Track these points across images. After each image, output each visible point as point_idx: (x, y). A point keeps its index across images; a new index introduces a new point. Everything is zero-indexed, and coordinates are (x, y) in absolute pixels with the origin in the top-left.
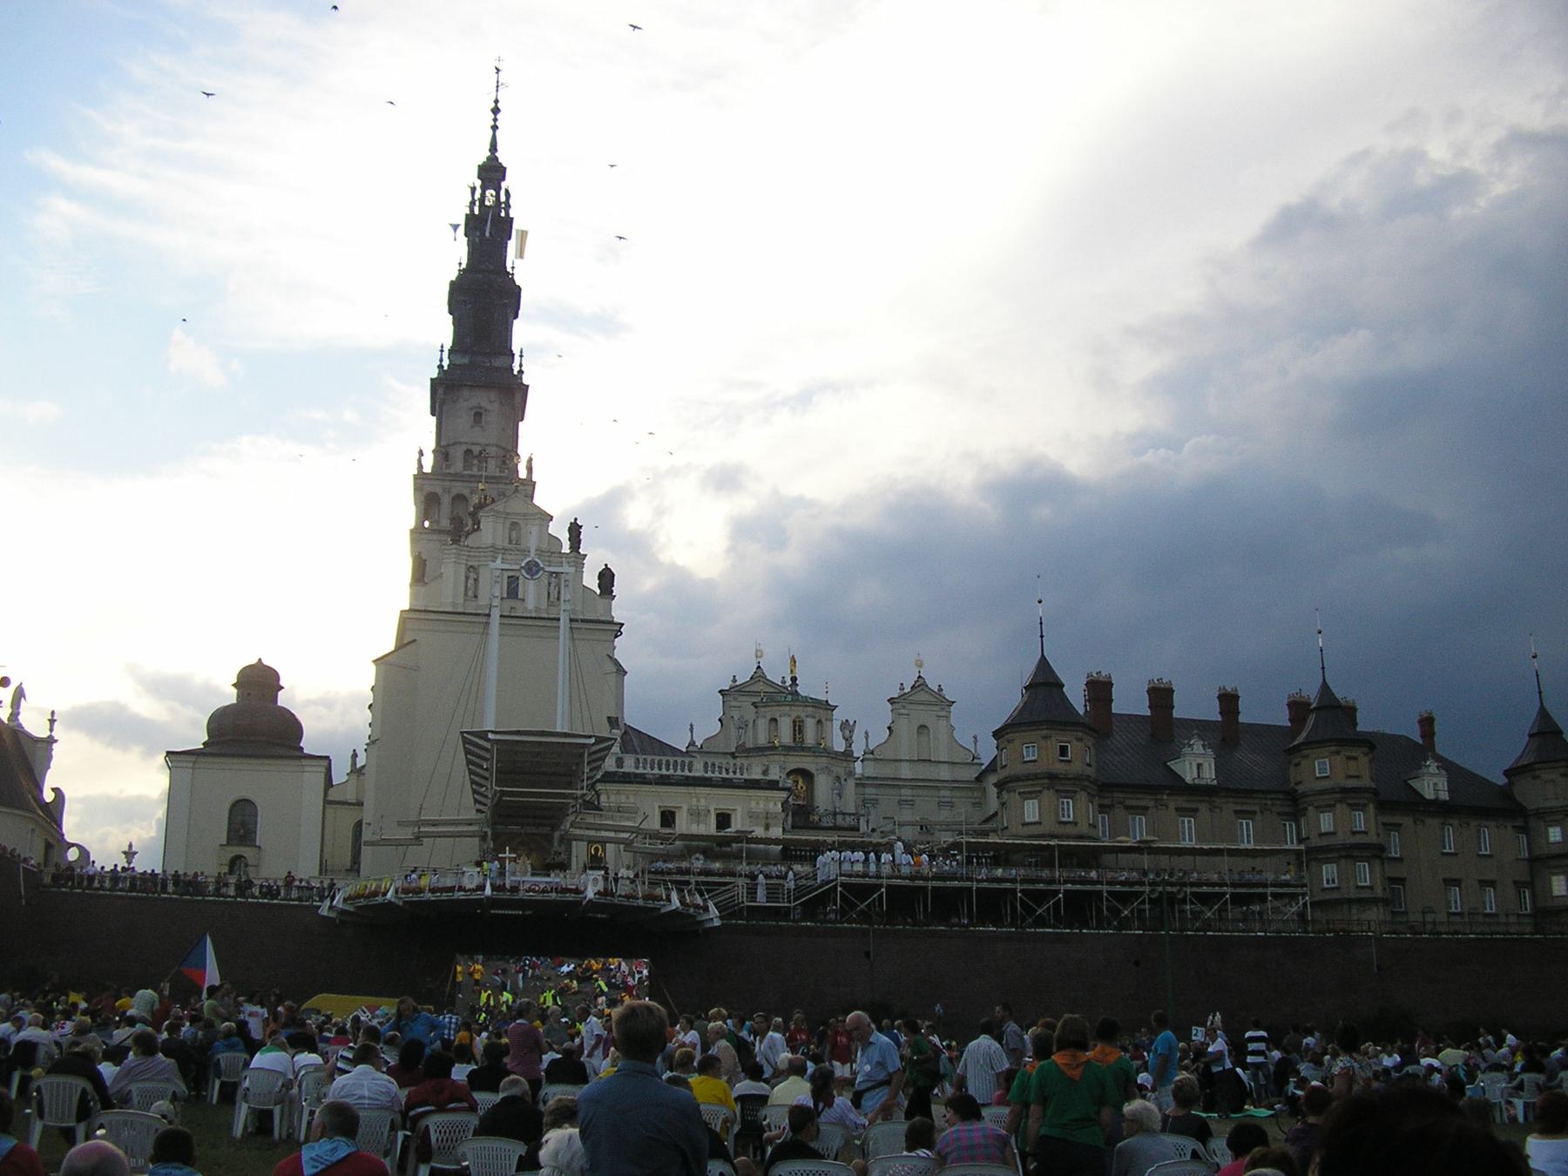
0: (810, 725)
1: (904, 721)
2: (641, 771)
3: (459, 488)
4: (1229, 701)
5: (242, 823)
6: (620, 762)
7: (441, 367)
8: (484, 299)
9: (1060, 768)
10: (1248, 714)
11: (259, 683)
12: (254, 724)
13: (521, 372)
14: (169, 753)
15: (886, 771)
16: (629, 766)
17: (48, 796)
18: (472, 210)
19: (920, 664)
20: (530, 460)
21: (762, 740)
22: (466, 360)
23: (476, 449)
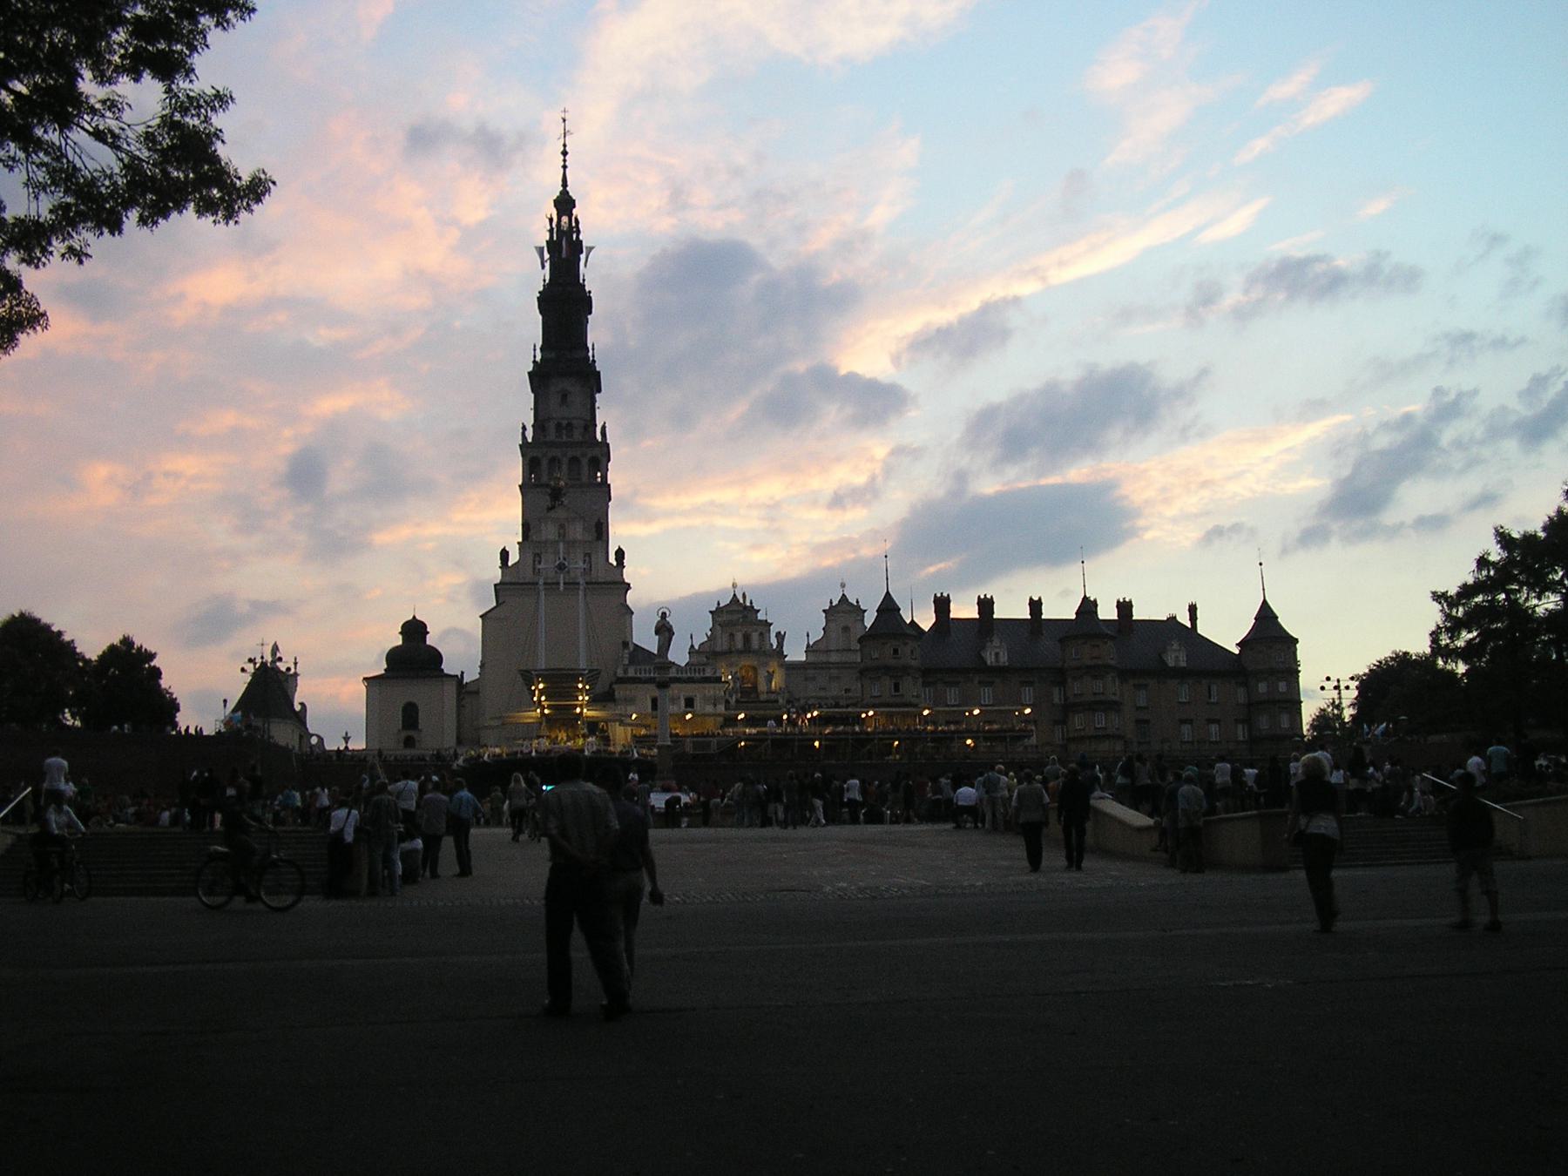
0: (755, 637)
1: (832, 625)
3: (556, 452)
4: (1036, 606)
5: (410, 715)
6: (625, 671)
8: (565, 303)
9: (892, 662)
10: (1048, 613)
11: (414, 630)
12: (414, 655)
15: (823, 658)
16: (631, 673)
17: (298, 708)
19: (843, 586)
20: (604, 428)
21: (725, 647)
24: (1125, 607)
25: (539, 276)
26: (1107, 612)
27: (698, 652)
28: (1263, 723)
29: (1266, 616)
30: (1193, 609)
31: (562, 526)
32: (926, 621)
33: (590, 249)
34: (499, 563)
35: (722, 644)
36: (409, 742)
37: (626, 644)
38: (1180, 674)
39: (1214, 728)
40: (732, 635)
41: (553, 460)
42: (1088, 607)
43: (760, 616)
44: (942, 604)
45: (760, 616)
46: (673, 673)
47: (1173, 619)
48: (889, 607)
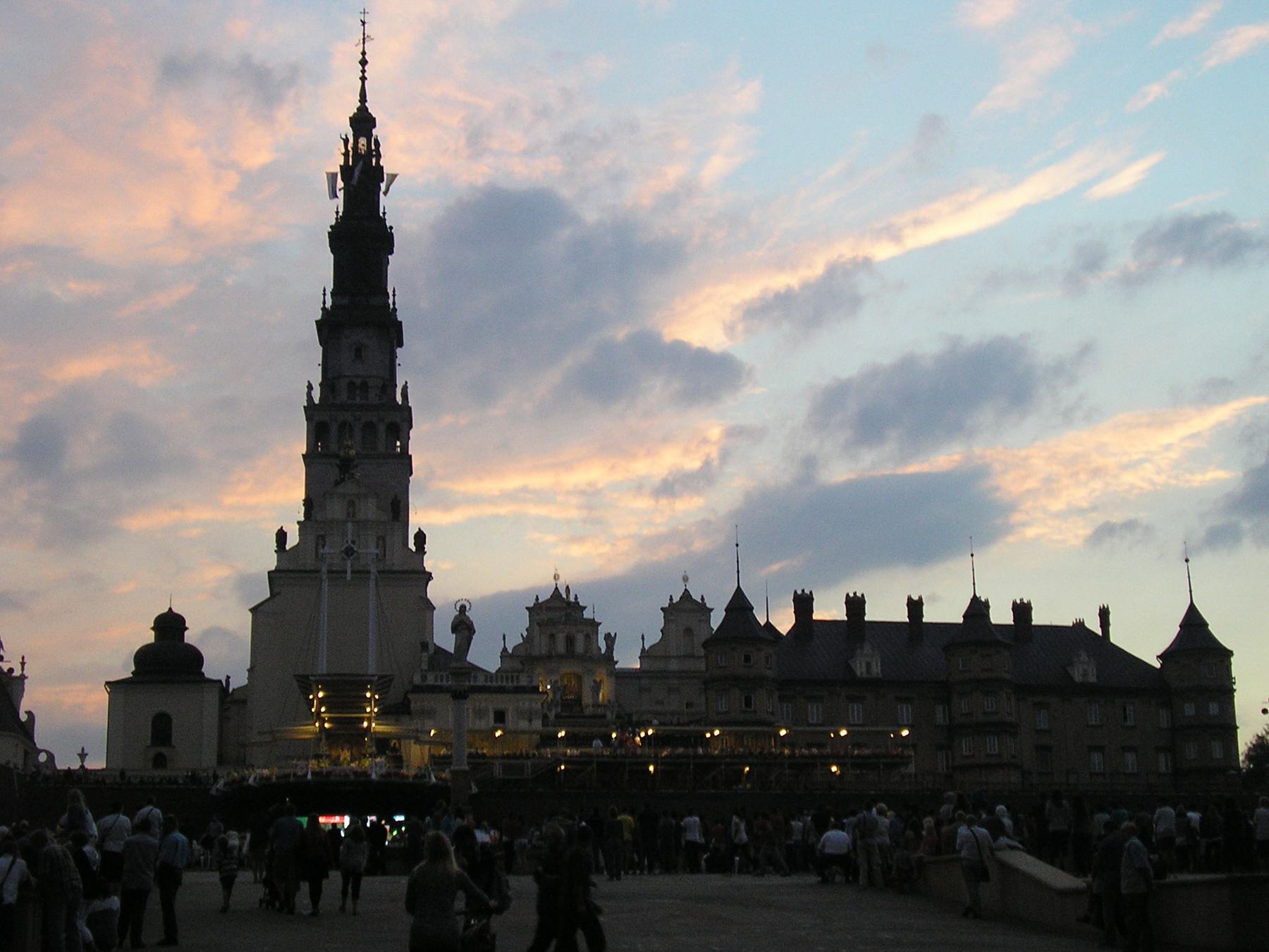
0: (580, 639)
2: (439, 683)
4: (915, 607)
5: (162, 728)
6: (424, 678)
7: (324, 309)
8: (361, 239)
11: (170, 625)
12: (168, 654)
13: (395, 310)
14: (107, 683)
15: (659, 665)
16: (431, 680)
17: (23, 717)
18: (346, 160)
19: (685, 579)
20: (405, 388)
22: (345, 301)
23: (358, 382)
24: (1022, 610)
25: (330, 209)
26: (1001, 615)
27: (511, 656)
28: (1191, 752)
29: (1193, 623)
30: (1104, 614)
31: (352, 503)
32: (784, 621)
33: (393, 177)
34: (274, 546)
35: (541, 647)
36: (160, 761)
37: (425, 646)
38: (1089, 691)
39: (1130, 758)
40: (552, 636)
41: (343, 426)
42: (978, 608)
43: (587, 614)
44: (803, 604)
45: (587, 614)
46: (481, 682)
47: (1080, 625)
48: (739, 606)
